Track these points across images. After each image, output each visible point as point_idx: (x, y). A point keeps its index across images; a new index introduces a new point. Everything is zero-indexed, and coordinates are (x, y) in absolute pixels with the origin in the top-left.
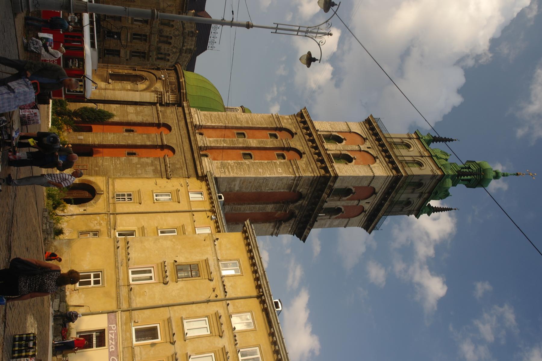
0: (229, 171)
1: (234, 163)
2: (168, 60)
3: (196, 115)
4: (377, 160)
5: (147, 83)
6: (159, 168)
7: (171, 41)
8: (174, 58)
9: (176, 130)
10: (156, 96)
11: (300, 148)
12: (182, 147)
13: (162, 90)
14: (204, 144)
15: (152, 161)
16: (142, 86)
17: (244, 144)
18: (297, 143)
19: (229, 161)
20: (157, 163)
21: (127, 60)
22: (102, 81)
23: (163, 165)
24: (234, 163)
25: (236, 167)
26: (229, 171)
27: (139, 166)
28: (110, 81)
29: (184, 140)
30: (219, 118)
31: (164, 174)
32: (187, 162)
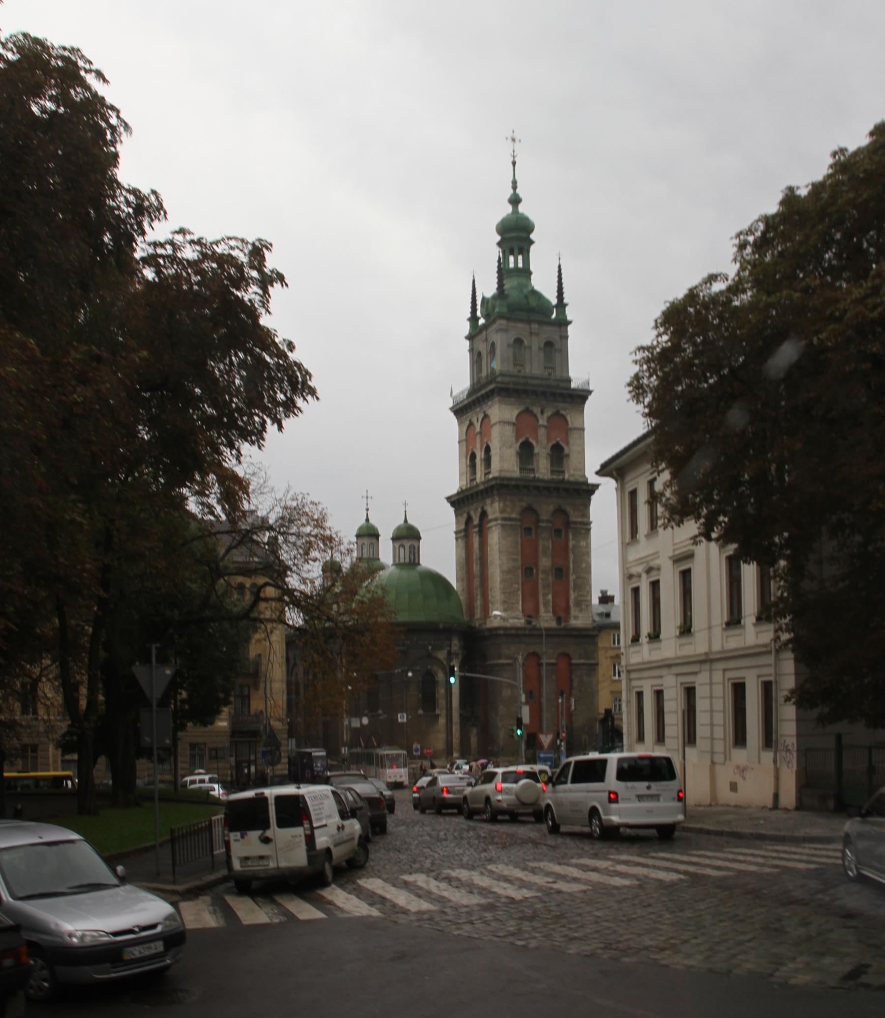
4: (563, 412)
5: (435, 668)
11: (551, 508)
13: (445, 652)
18: (546, 509)
28: (437, 712)
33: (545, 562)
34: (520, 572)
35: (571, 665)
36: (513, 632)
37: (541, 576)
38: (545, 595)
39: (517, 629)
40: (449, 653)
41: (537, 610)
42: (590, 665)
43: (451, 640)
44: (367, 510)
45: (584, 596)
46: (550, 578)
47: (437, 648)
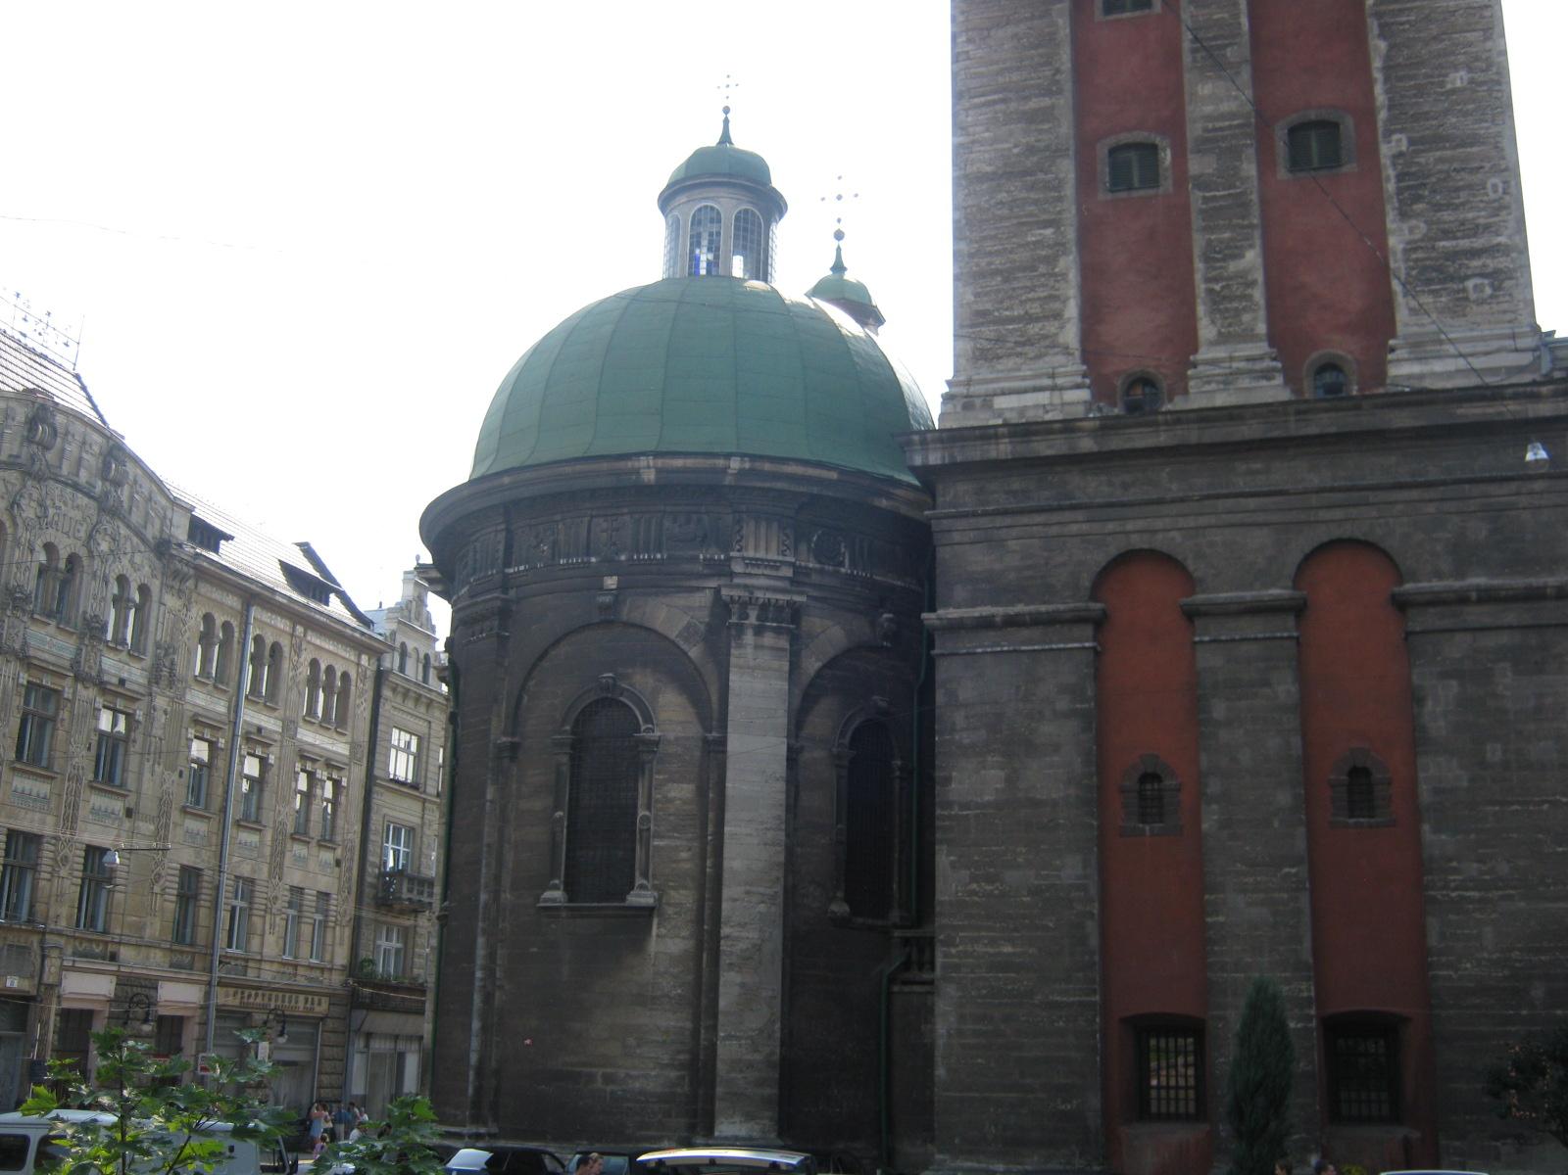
0: (1475, 253)
1: (1404, 215)
2: (144, 590)
3: (1001, 403)
5: (642, 681)
6: (1504, 639)
7: (64, 554)
8: (138, 558)
9: (1159, 524)
10: (749, 638)
12: (1314, 500)
13: (702, 600)
14: (1267, 374)
15: (1445, 675)
16: (671, 717)
19: (1396, 243)
20: (1457, 648)
21: (129, 813)
23: (1475, 615)
24: (1404, 215)
25: (1438, 207)
26: (1475, 253)
27: (1494, 752)
29: (1241, 483)
30: (1008, 275)
32: (1433, 473)
33: (1215, 99)
34: (1067, 169)
35: (1402, 605)
36: (1003, 449)
37: (1196, 165)
38: (1218, 255)
40: (721, 607)
44: (839, 235)
45: (1476, 230)
47: (665, 581)
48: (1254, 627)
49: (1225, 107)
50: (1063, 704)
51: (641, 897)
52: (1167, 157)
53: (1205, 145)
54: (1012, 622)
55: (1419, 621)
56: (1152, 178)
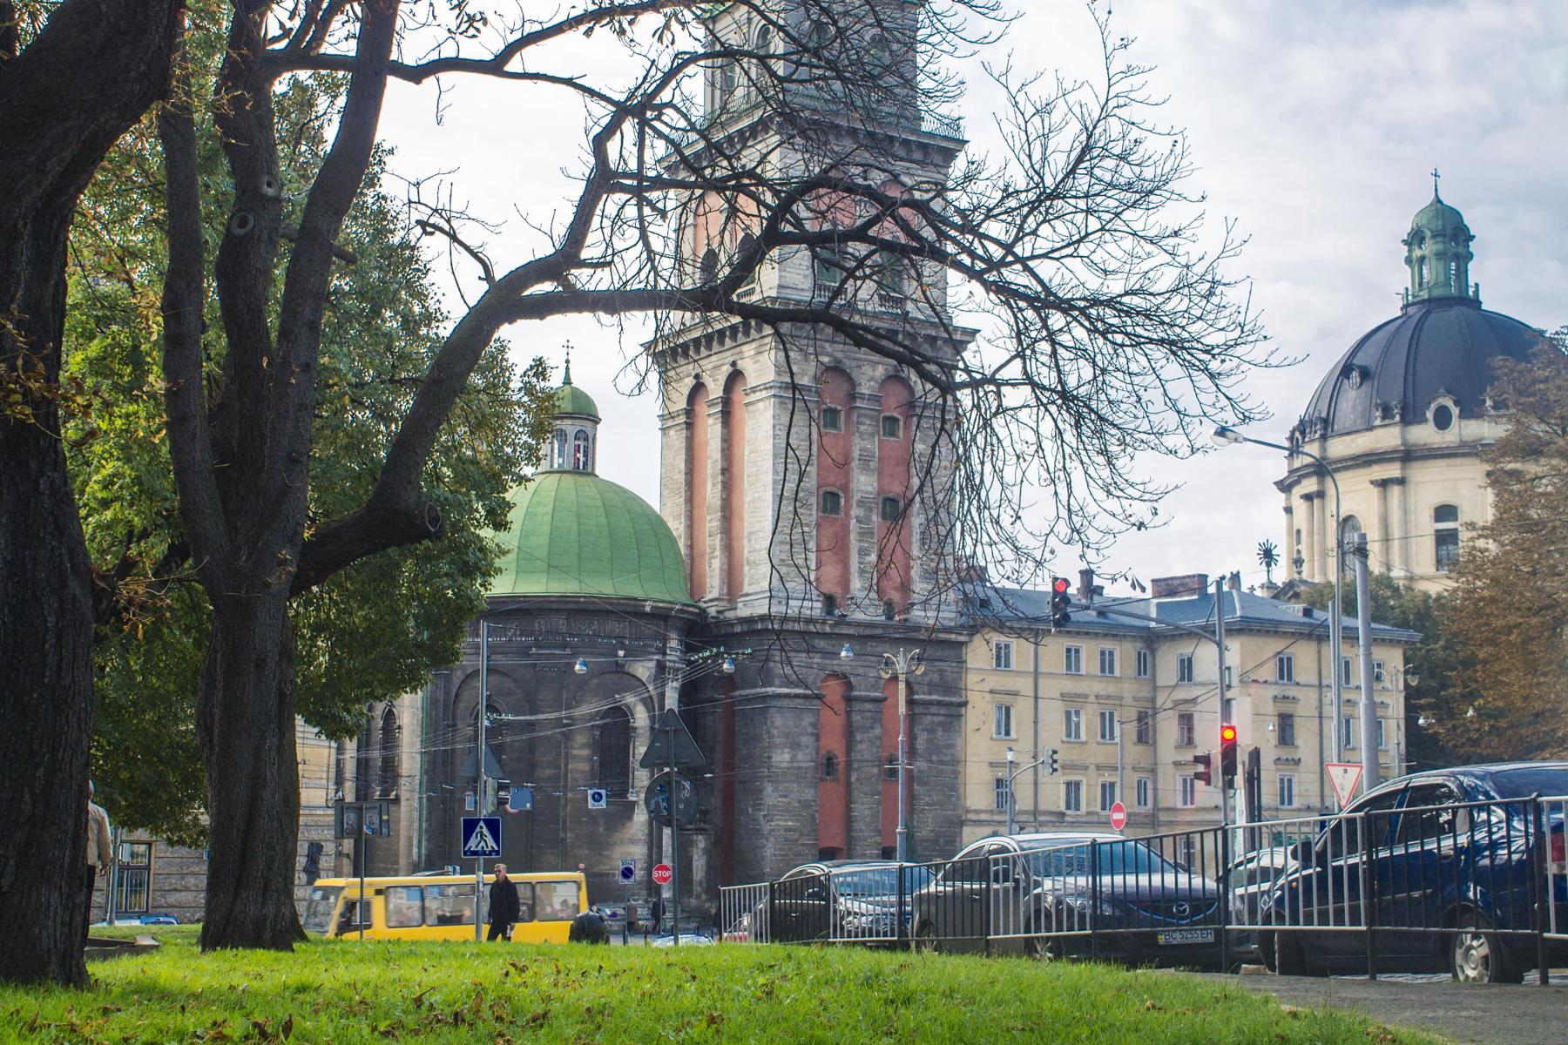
11: (880, 371)
13: (653, 664)
17: (871, 510)
20: (927, 720)
22: (630, 818)
23: (933, 709)
31: (953, 711)
37: (856, 511)
39: (810, 621)
40: (661, 667)
41: (845, 582)
42: (951, 704)
43: (665, 640)
46: (875, 518)
47: (635, 653)
48: (868, 706)
49: (870, 489)
50: (810, 730)
51: (632, 798)
52: (843, 501)
53: (861, 503)
54: (797, 696)
55: (919, 710)
56: (835, 509)
